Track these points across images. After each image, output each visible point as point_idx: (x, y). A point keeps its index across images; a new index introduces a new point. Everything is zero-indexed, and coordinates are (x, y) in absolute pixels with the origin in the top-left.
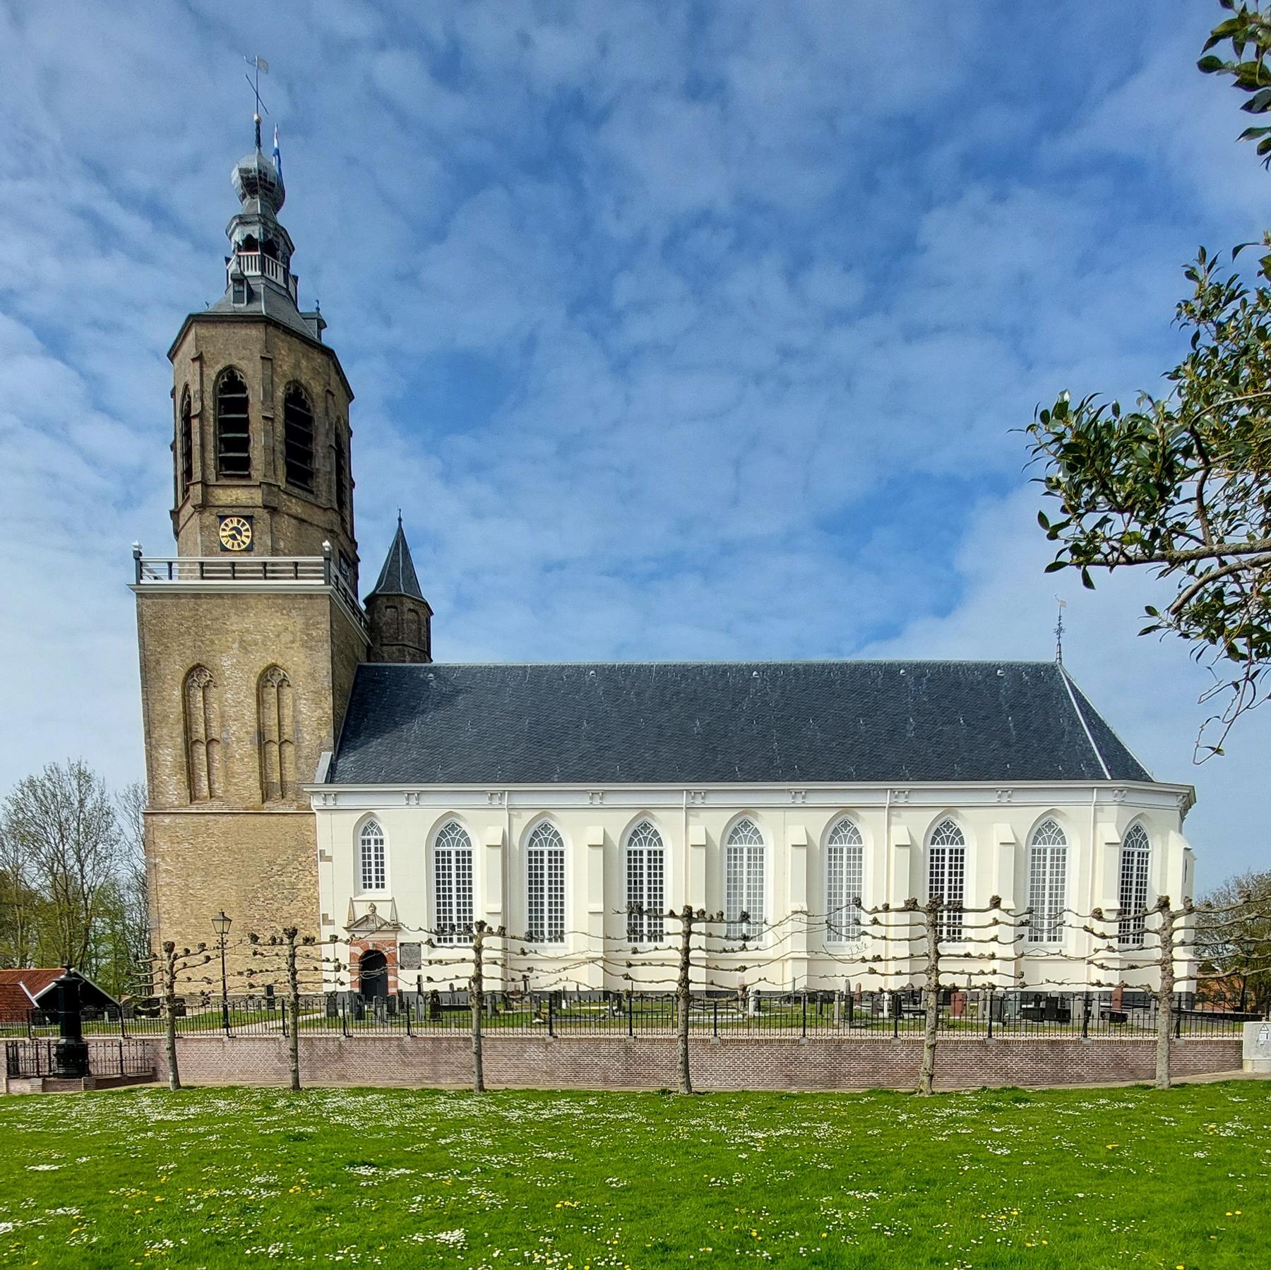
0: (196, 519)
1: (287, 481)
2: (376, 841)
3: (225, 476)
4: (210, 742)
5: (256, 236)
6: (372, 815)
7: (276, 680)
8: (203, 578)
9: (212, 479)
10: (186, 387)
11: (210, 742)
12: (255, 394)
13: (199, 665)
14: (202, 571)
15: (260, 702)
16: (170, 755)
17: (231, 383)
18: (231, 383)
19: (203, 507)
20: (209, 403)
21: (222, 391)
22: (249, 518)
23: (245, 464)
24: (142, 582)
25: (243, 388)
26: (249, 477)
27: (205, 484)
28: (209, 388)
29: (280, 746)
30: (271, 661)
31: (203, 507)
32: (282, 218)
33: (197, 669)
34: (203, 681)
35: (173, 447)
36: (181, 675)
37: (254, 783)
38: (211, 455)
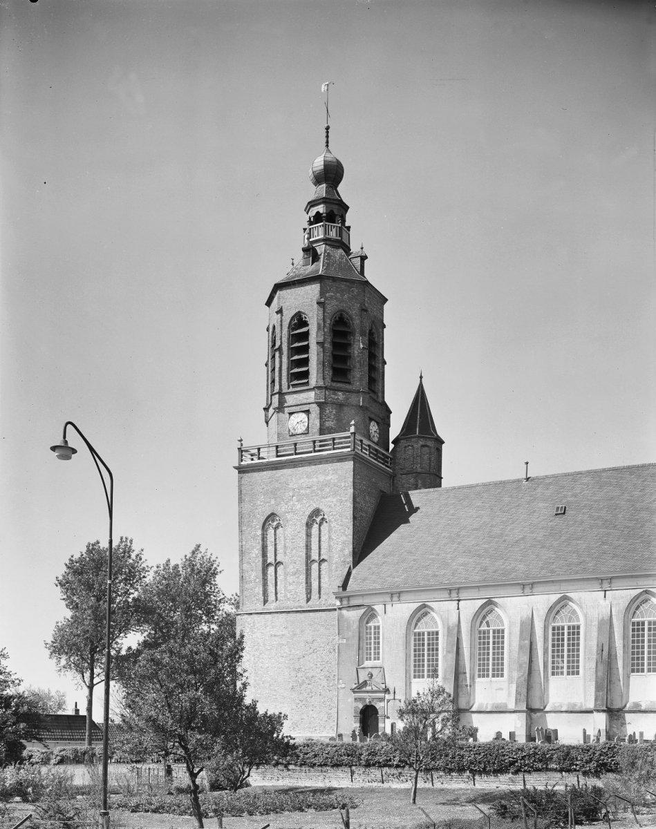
0: (275, 414)
1: (332, 381)
2: (375, 627)
3: (294, 386)
4: (278, 564)
5: (321, 212)
6: (373, 609)
7: (318, 520)
8: (278, 456)
9: (285, 390)
10: (274, 327)
11: (278, 564)
12: (313, 329)
13: (273, 514)
14: (277, 452)
15: (309, 535)
16: (255, 575)
17: (299, 321)
18: (299, 321)
19: (280, 409)
20: (285, 340)
21: (294, 329)
22: (307, 412)
23: (306, 375)
24: (242, 463)
25: (305, 324)
26: (307, 383)
27: (281, 393)
28: (286, 324)
29: (320, 565)
30: (315, 506)
31: (280, 409)
32: (342, 188)
33: (272, 516)
34: (275, 523)
35: (266, 365)
36: (259, 526)
37: (302, 589)
38: (284, 373)
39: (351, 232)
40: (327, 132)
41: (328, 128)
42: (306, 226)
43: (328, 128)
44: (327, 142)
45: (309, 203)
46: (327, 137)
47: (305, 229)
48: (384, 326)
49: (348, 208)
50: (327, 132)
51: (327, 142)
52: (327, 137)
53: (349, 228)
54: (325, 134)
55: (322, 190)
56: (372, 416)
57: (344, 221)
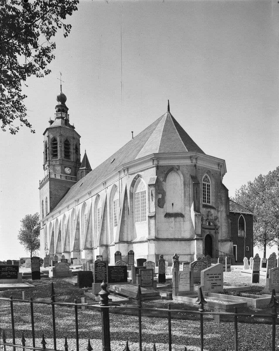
39: (69, 116)
40: (61, 87)
41: (61, 86)
42: (56, 113)
43: (61, 86)
44: (61, 90)
45: (56, 106)
46: (61, 88)
47: (55, 114)
48: (80, 144)
49: (68, 109)
50: (61, 87)
51: (61, 90)
52: (61, 88)
53: (69, 115)
54: (60, 87)
55: (60, 103)
56: (66, 166)
57: (67, 113)
